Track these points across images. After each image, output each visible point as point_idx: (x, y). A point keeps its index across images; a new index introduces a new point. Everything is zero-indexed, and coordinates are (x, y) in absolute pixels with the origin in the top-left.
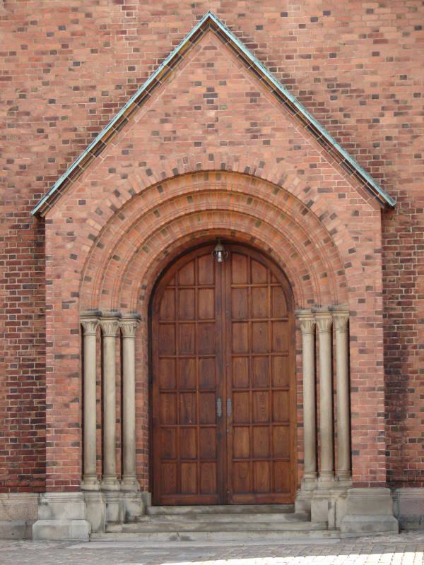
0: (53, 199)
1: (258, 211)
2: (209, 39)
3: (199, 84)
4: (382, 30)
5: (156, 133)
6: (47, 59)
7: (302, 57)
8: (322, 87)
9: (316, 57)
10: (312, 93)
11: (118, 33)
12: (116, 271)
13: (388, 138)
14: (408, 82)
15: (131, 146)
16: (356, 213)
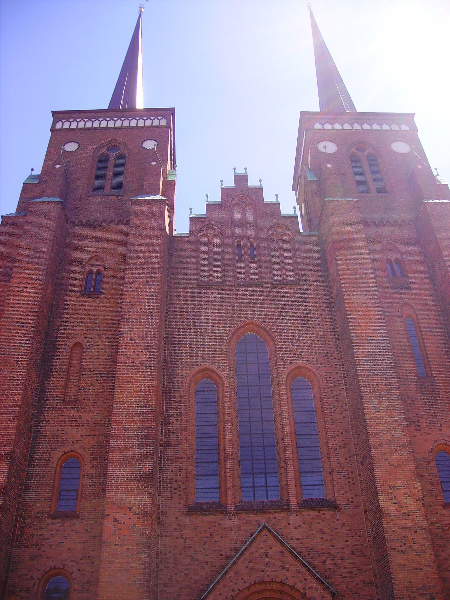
0: (209, 593)
2: (265, 532)
3: (262, 548)
4: (323, 529)
5: (247, 567)
6: (205, 540)
7: (296, 539)
8: (304, 550)
9: (301, 539)
10: (301, 552)
11: (230, 530)
13: (329, 569)
14: (334, 548)
15: (238, 572)
16: (323, 597)
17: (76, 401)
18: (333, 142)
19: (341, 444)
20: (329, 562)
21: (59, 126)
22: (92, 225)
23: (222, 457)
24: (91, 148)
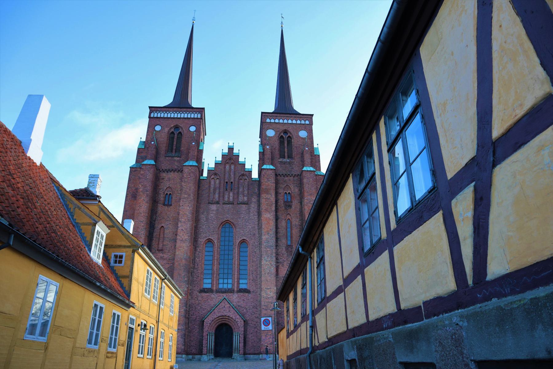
1: (229, 321)
2: (225, 300)
6: (205, 301)
12: (212, 327)
17: (162, 250)
18: (273, 130)
19: (255, 270)
20: (245, 310)
21: (152, 116)
22: (167, 172)
23: (213, 273)
24: (166, 130)
